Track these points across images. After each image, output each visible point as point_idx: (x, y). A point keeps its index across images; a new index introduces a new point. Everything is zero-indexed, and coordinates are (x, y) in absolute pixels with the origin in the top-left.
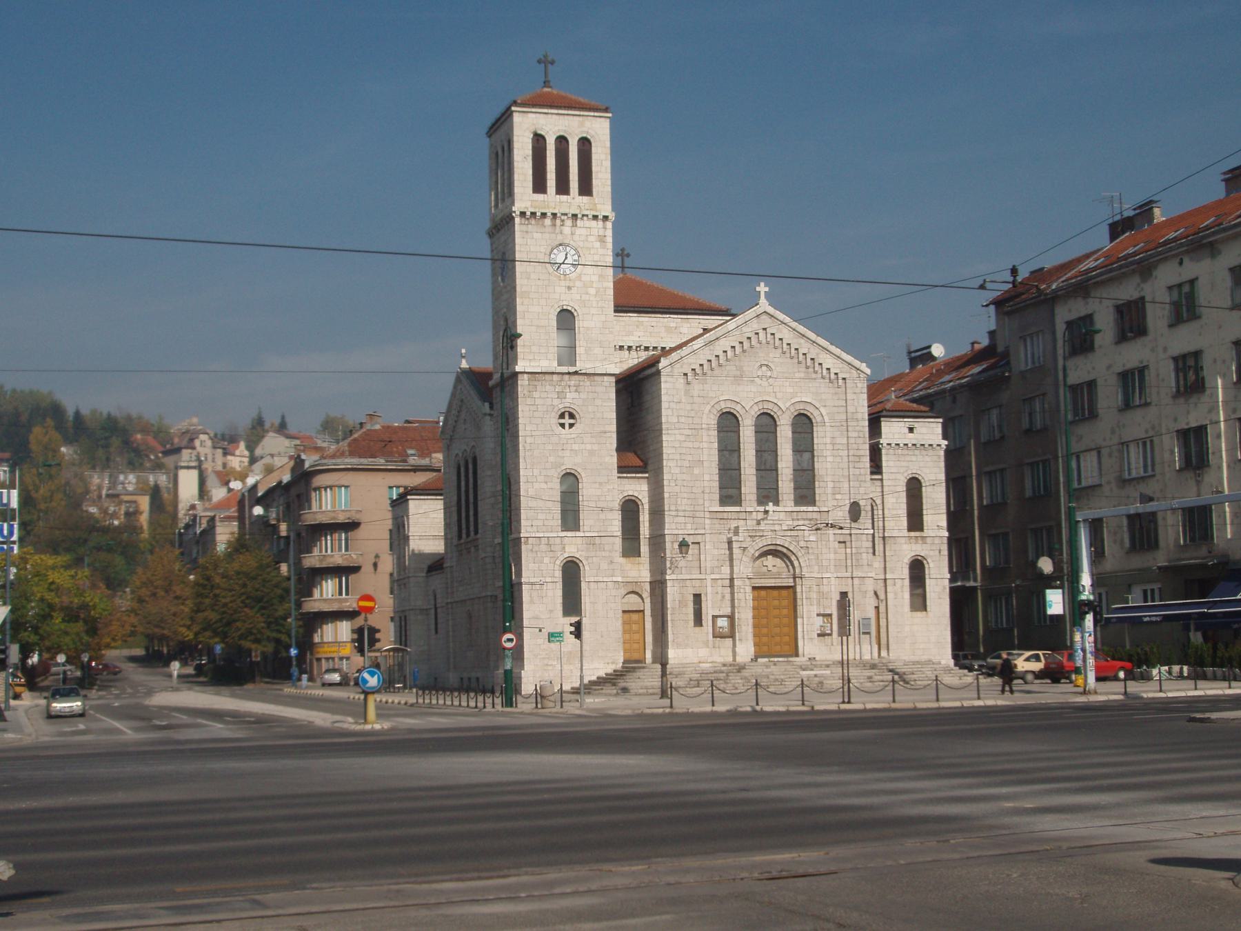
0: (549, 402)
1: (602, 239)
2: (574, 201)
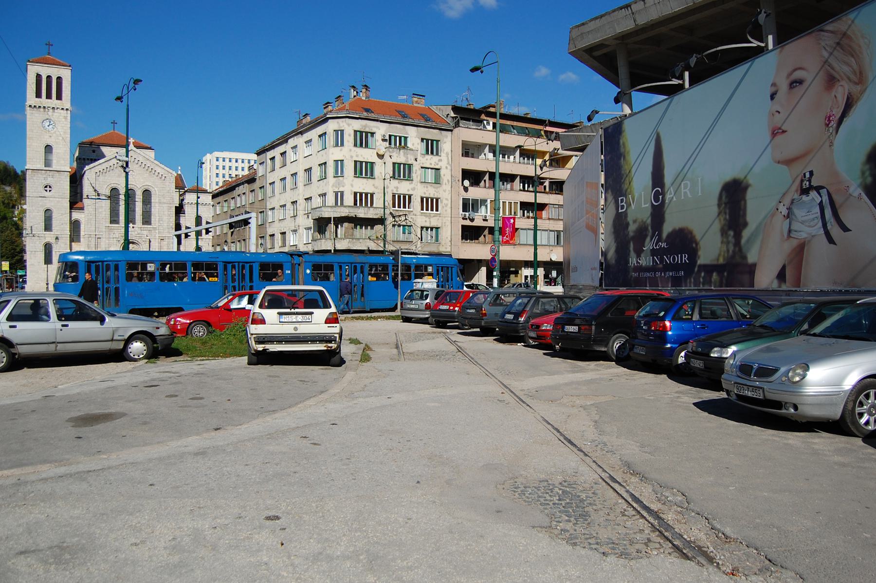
0: (40, 181)
1: (65, 118)
2: (54, 102)
